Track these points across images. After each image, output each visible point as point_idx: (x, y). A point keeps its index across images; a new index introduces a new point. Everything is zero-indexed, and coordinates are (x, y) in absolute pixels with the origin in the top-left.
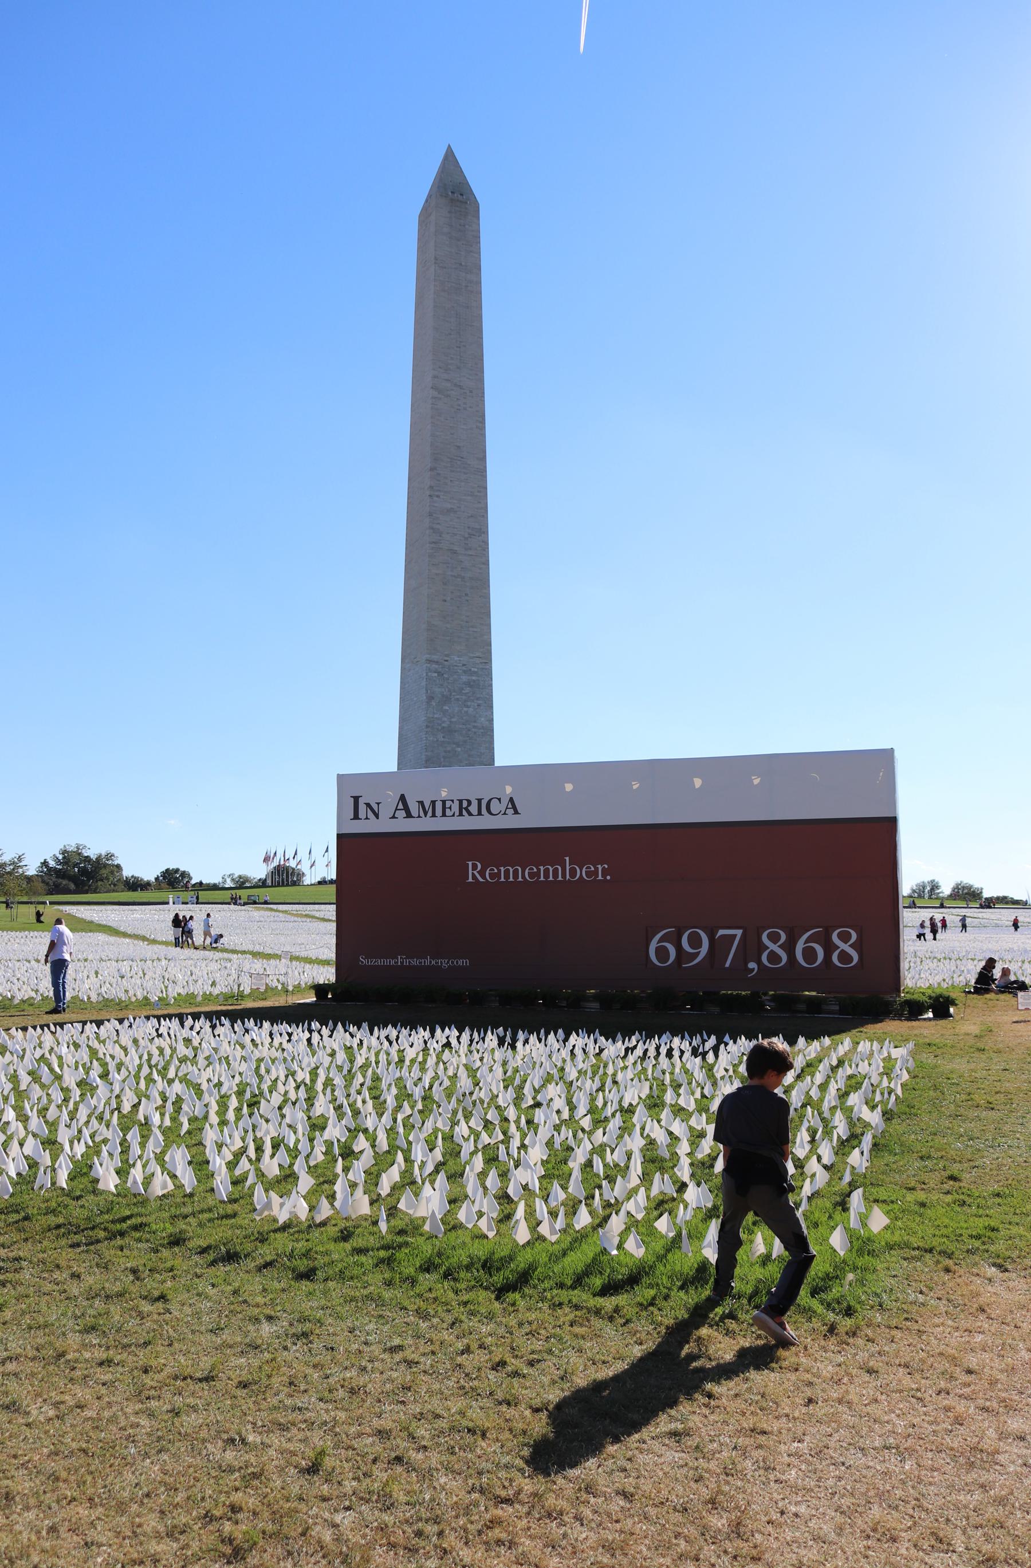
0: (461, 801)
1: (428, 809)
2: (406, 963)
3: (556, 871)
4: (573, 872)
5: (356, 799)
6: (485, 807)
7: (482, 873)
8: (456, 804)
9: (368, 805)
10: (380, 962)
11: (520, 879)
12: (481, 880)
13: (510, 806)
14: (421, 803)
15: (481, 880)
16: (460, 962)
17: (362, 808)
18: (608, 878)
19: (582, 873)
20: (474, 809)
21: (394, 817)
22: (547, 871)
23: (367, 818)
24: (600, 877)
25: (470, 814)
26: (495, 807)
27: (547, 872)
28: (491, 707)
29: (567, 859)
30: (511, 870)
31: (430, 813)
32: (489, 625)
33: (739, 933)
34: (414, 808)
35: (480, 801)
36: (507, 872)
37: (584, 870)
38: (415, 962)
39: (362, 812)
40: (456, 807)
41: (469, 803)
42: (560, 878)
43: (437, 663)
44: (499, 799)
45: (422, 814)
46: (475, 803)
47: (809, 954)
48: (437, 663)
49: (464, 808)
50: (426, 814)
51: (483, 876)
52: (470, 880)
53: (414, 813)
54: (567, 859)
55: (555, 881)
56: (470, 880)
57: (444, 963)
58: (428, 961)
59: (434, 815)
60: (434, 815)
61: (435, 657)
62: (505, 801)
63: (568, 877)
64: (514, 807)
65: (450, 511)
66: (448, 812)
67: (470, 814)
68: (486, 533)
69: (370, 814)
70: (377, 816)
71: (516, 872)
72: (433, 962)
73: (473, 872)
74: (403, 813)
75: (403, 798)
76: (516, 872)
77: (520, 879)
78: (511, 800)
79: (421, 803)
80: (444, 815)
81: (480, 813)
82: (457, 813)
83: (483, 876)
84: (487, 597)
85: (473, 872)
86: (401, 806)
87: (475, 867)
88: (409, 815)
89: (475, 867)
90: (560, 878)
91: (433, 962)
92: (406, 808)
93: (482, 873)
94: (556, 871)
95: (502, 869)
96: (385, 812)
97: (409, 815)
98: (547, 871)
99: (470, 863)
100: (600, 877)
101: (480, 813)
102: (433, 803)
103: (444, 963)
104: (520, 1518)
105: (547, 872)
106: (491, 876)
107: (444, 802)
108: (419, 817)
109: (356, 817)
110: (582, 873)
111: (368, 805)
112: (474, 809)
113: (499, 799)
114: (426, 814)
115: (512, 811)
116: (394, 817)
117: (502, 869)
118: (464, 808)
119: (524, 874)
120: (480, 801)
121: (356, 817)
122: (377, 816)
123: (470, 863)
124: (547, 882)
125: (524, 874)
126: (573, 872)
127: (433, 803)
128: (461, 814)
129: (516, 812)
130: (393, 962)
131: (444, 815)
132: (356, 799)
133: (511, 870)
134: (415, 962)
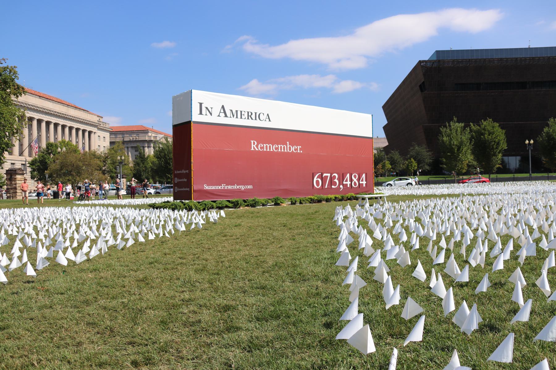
0: (248, 112)
1: (235, 114)
3: (284, 147)
5: (201, 104)
6: (258, 117)
8: (247, 113)
9: (207, 108)
10: (213, 188)
11: (272, 150)
14: (231, 111)
17: (204, 110)
19: (293, 149)
20: (253, 116)
21: (219, 116)
25: (252, 119)
35: (256, 113)
36: (267, 146)
38: (230, 187)
45: (232, 116)
46: (254, 114)
49: (249, 116)
50: (233, 116)
51: (258, 148)
53: (228, 115)
55: (284, 152)
56: (252, 149)
57: (243, 188)
58: (236, 187)
59: (237, 117)
60: (237, 117)
62: (266, 115)
64: (269, 118)
67: (252, 119)
70: (211, 114)
71: (270, 146)
72: (238, 187)
73: (254, 146)
74: (223, 115)
75: (223, 107)
76: (270, 146)
78: (268, 115)
79: (231, 111)
80: (241, 118)
81: (256, 119)
83: (258, 148)
86: (222, 111)
87: (254, 143)
88: (226, 116)
89: (254, 143)
91: (238, 187)
92: (225, 112)
93: (257, 146)
94: (284, 147)
95: (265, 145)
97: (226, 116)
101: (256, 119)
102: (237, 111)
103: (243, 188)
107: (241, 112)
109: (201, 113)
110: (293, 149)
111: (207, 108)
112: (253, 116)
114: (233, 116)
115: (268, 120)
116: (219, 116)
117: (265, 145)
120: (256, 113)
121: (201, 113)
122: (211, 114)
123: (252, 141)
124: (281, 152)
126: (290, 147)
127: (237, 111)
128: (248, 118)
129: (270, 121)
130: (220, 188)
131: (241, 118)
132: (201, 104)
134: (230, 187)
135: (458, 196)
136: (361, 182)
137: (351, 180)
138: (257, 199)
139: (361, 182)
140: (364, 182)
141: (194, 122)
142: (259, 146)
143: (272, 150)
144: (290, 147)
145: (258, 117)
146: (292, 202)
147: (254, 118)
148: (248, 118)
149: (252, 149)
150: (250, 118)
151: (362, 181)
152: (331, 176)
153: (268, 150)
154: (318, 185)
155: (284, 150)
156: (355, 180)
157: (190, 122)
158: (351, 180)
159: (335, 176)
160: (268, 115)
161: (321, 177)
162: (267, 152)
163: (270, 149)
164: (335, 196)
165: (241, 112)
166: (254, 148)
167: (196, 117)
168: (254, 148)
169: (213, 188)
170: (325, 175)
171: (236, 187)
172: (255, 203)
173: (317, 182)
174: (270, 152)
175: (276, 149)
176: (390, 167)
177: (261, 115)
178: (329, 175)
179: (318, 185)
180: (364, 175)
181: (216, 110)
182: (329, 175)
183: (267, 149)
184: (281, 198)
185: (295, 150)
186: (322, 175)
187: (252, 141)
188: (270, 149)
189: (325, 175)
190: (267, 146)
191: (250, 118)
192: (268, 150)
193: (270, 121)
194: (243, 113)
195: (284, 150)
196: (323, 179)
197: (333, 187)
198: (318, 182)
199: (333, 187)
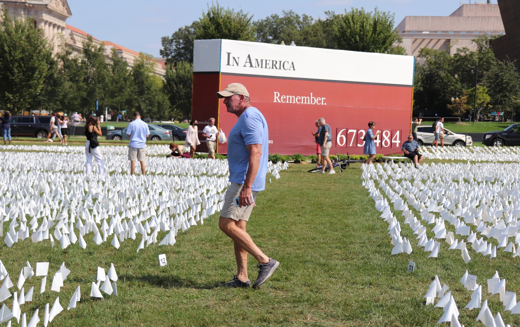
0: (273, 61)
1: (261, 63)
3: (307, 99)
4: (313, 102)
5: (229, 54)
6: (282, 65)
7: (280, 98)
8: (271, 62)
9: (234, 58)
11: (294, 102)
14: (257, 60)
18: (325, 104)
19: (316, 101)
20: (278, 66)
21: (245, 66)
25: (276, 68)
29: (311, 94)
30: (291, 98)
31: (260, 66)
35: (280, 62)
39: (231, 63)
45: (257, 66)
46: (278, 63)
49: (274, 66)
50: (258, 65)
54: (311, 94)
55: (307, 105)
56: (275, 101)
59: (262, 67)
60: (262, 67)
62: (290, 63)
63: (311, 103)
64: (293, 67)
67: (276, 68)
70: (237, 64)
71: (293, 98)
75: (249, 56)
76: (293, 98)
78: (293, 63)
79: (257, 60)
80: (266, 67)
81: (280, 68)
82: (271, 67)
83: (280, 100)
86: (248, 61)
88: (251, 66)
90: (309, 103)
93: (280, 98)
94: (307, 99)
95: (288, 97)
96: (242, 62)
97: (251, 66)
100: (322, 104)
101: (280, 68)
102: (262, 60)
106: (284, 100)
107: (266, 61)
109: (228, 64)
110: (316, 101)
111: (234, 58)
112: (278, 66)
114: (258, 65)
115: (292, 69)
116: (245, 66)
120: (280, 62)
121: (228, 64)
122: (237, 64)
123: (275, 93)
126: (313, 99)
127: (262, 60)
128: (273, 68)
129: (294, 69)
131: (266, 67)
132: (229, 54)
133: (291, 98)
135: (509, 162)
136: (393, 141)
137: (382, 138)
138: (279, 155)
139: (393, 141)
140: (398, 142)
141: (223, 73)
143: (294, 102)
144: (313, 99)
145: (282, 65)
146: (312, 160)
147: (278, 67)
148: (273, 68)
149: (275, 101)
151: (396, 139)
152: (357, 132)
153: (291, 102)
154: (342, 142)
155: (307, 102)
156: (386, 138)
157: (217, 74)
158: (382, 138)
159: (362, 133)
160: (293, 63)
161: (346, 133)
162: (289, 104)
163: (293, 101)
164: (361, 156)
165: (266, 61)
167: (224, 68)
170: (350, 131)
172: (276, 160)
173: (341, 139)
174: (292, 104)
175: (299, 101)
176: (488, 99)
177: (286, 64)
178: (355, 131)
179: (342, 142)
180: (398, 133)
181: (243, 60)
182: (355, 131)
183: (289, 101)
184: (302, 155)
185: (319, 102)
186: (347, 131)
187: (275, 93)
188: (293, 101)
189: (350, 131)
192: (291, 102)
193: (294, 69)
194: (268, 62)
195: (307, 102)
196: (348, 136)
197: (359, 145)
198: (341, 139)
199: (359, 145)
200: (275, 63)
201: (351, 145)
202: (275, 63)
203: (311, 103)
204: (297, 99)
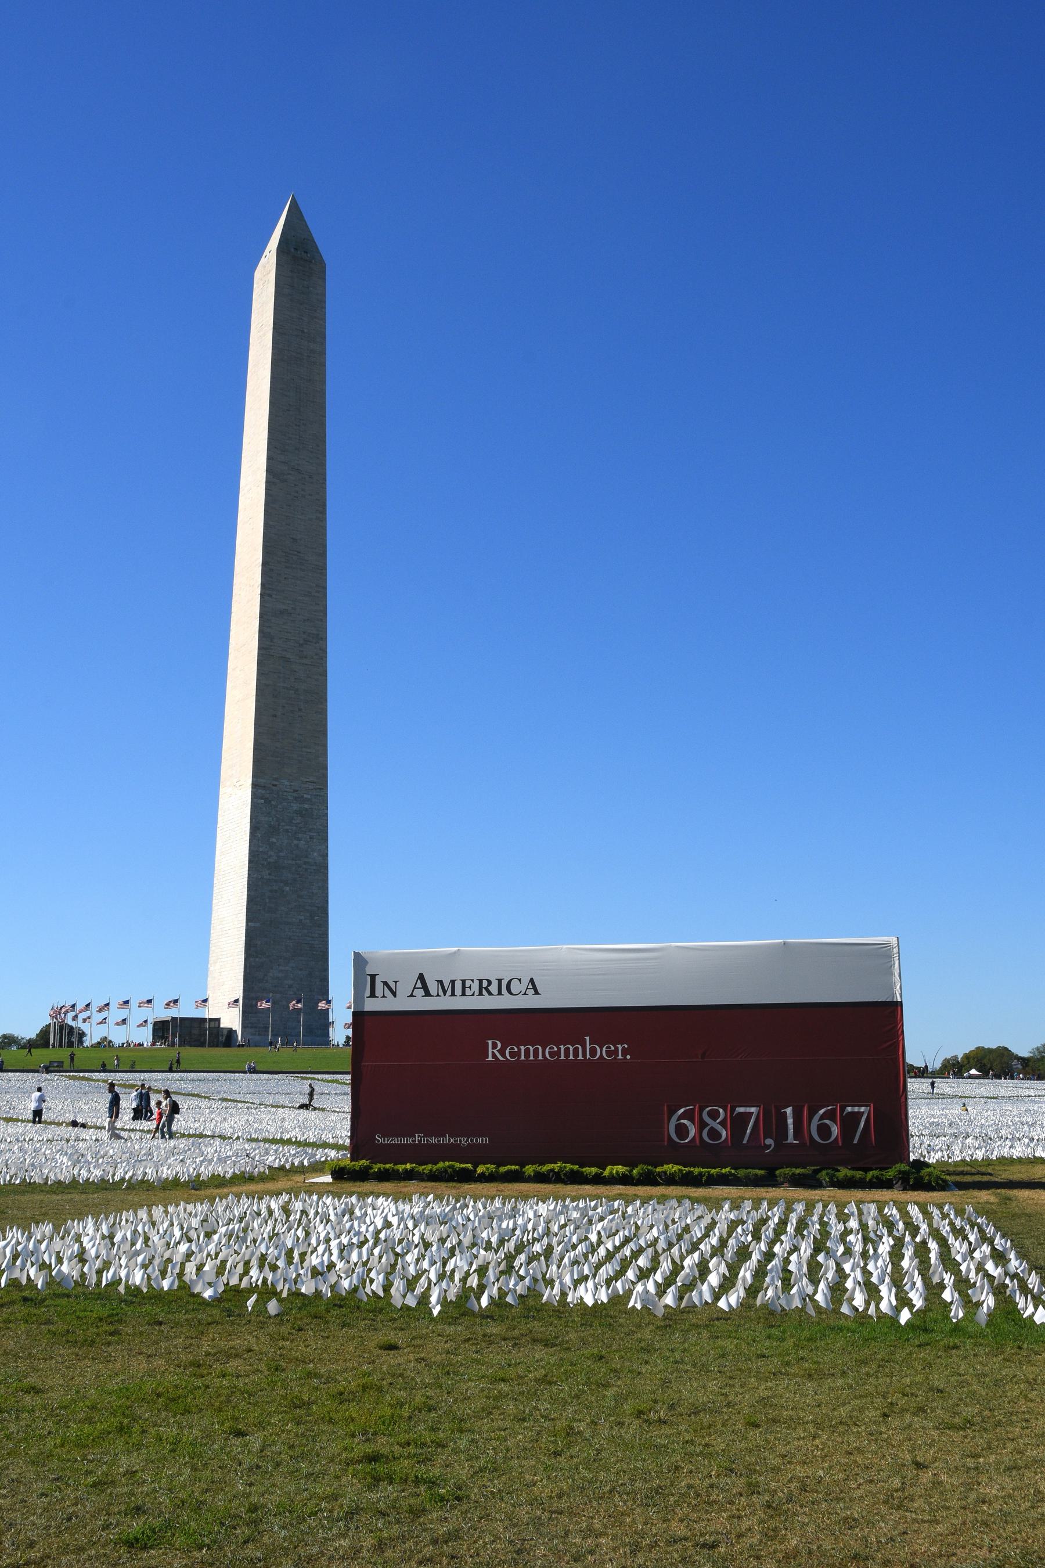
0: (481, 981)
1: (447, 988)
2: (424, 1140)
3: (576, 1051)
4: (593, 1052)
5: (373, 977)
6: (506, 987)
7: (502, 1052)
8: (477, 983)
9: (385, 983)
10: (397, 1141)
11: (540, 1058)
12: (501, 1058)
13: (530, 986)
15: (501, 1058)
16: (480, 1140)
17: (379, 986)
19: (602, 1052)
20: (494, 988)
21: (412, 996)
22: (567, 1051)
23: (384, 996)
24: (620, 1057)
25: (490, 994)
26: (514, 988)
27: (567, 1052)
28: (325, 840)
29: (588, 1038)
31: (449, 992)
32: (325, 746)
33: (753, 1110)
34: (433, 988)
35: (500, 981)
37: (604, 1049)
38: (433, 1140)
39: (379, 991)
40: (475, 987)
41: (489, 982)
42: (580, 1057)
43: (264, 787)
44: (520, 980)
45: (441, 993)
46: (495, 984)
47: (824, 1131)
48: (264, 787)
50: (445, 992)
51: (503, 1055)
52: (490, 1058)
53: (433, 990)
54: (588, 1038)
56: (490, 1058)
57: (464, 1141)
58: (446, 1140)
59: (453, 994)
60: (453, 994)
61: (262, 781)
62: (526, 981)
63: (588, 1056)
64: (535, 988)
65: (282, 612)
66: (468, 991)
67: (490, 994)
68: (324, 639)
69: (387, 992)
70: (394, 994)
71: (536, 1051)
72: (452, 1140)
74: (422, 992)
75: (421, 977)
76: (536, 1051)
77: (540, 1058)
78: (532, 981)
79: (441, 982)
80: (464, 994)
81: (500, 993)
82: (477, 993)
83: (503, 1055)
84: (323, 713)
85: (493, 1050)
86: (419, 985)
87: (494, 1046)
88: (427, 994)
89: (494, 1046)
90: (580, 1057)
91: (452, 1140)
93: (502, 1052)
94: (576, 1051)
95: (522, 1048)
96: (403, 990)
97: (427, 994)
98: (567, 1051)
99: (490, 1042)
100: (620, 1057)
101: (500, 993)
103: (464, 1141)
104: (912, 1451)
105: (567, 1052)
106: (512, 1054)
107: (464, 981)
108: (438, 995)
109: (373, 995)
110: (602, 1052)
112: (494, 988)
113: (520, 980)
114: (445, 992)
115: (531, 992)
116: (412, 996)
117: (522, 1048)
118: (484, 988)
119: (545, 1053)
120: (500, 981)
121: (373, 995)
122: (394, 994)
123: (490, 1042)
125: (545, 1053)
126: (593, 1052)
127: (453, 982)
128: (481, 994)
129: (537, 993)
130: (410, 1141)
131: (464, 994)
134: (433, 1140)
142: (508, 1051)
148: (481, 994)
150: (484, 992)
165: (464, 981)
166: (494, 1054)
168: (494, 1054)
169: (397, 1141)
171: (446, 1140)
175: (551, 1054)
185: (608, 1053)
190: (527, 1051)
191: (484, 992)
193: (537, 993)
198: (682, 1131)
200: (485, 984)
201: (856, 1141)
202: (485, 984)
203: (588, 1056)
204: (547, 1050)
